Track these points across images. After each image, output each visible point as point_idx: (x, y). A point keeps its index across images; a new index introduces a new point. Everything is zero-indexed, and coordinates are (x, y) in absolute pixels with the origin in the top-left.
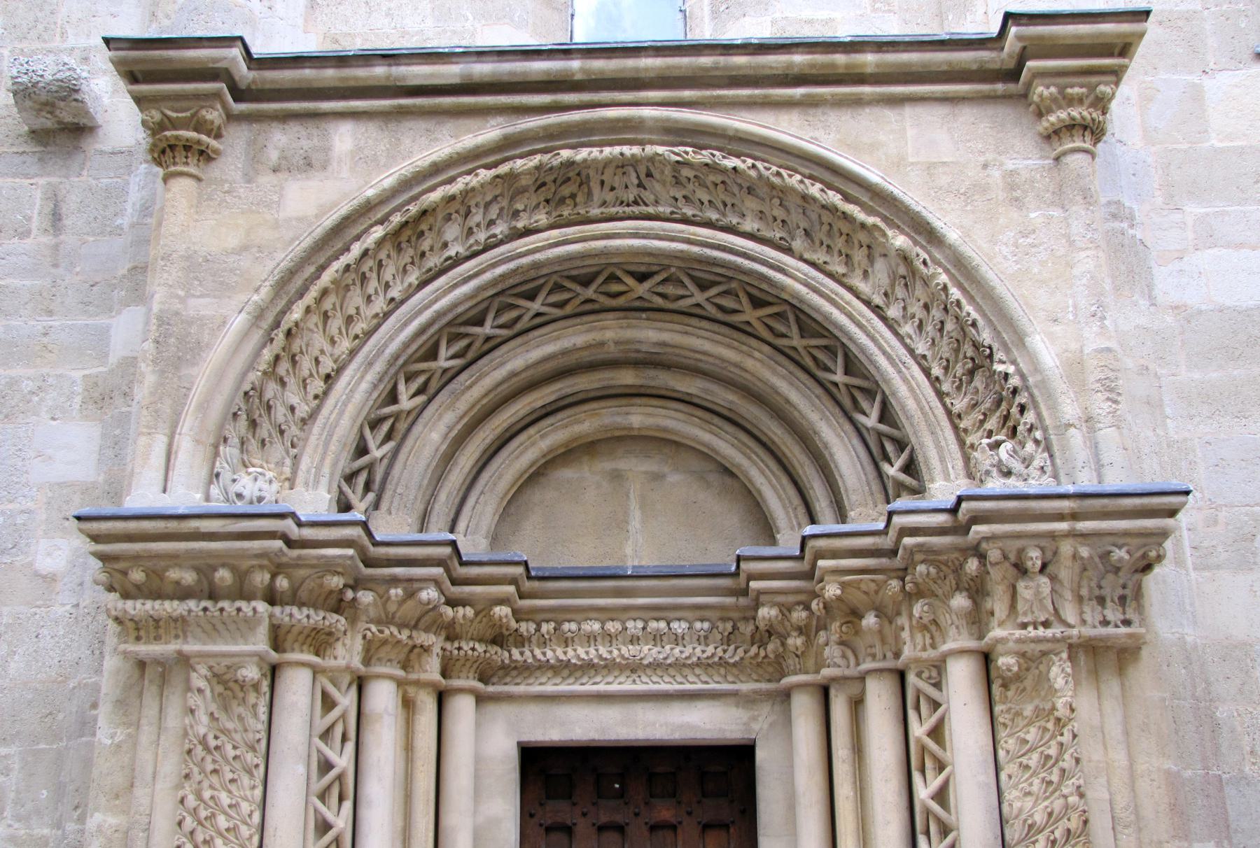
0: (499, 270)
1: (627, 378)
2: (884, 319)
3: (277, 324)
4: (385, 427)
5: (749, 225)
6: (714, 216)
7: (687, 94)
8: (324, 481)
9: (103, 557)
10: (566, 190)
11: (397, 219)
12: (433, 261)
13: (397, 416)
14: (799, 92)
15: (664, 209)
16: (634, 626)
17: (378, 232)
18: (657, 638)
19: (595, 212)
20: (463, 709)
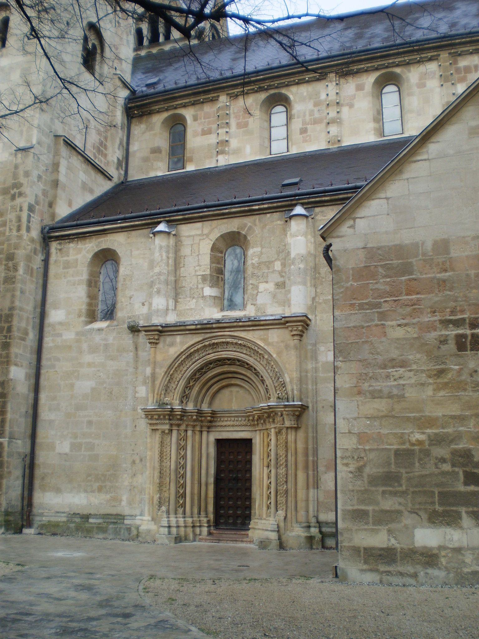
0: (204, 362)
1: (230, 375)
2: (265, 369)
3: (169, 374)
4: (189, 388)
5: (244, 352)
6: (238, 350)
7: (232, 329)
8: (178, 400)
9: (145, 415)
10: (215, 347)
11: (186, 355)
12: (194, 360)
13: (190, 386)
14: (251, 328)
15: (231, 349)
16: (233, 419)
17: (184, 357)
18: (237, 421)
19: (219, 350)
20: (205, 434)
